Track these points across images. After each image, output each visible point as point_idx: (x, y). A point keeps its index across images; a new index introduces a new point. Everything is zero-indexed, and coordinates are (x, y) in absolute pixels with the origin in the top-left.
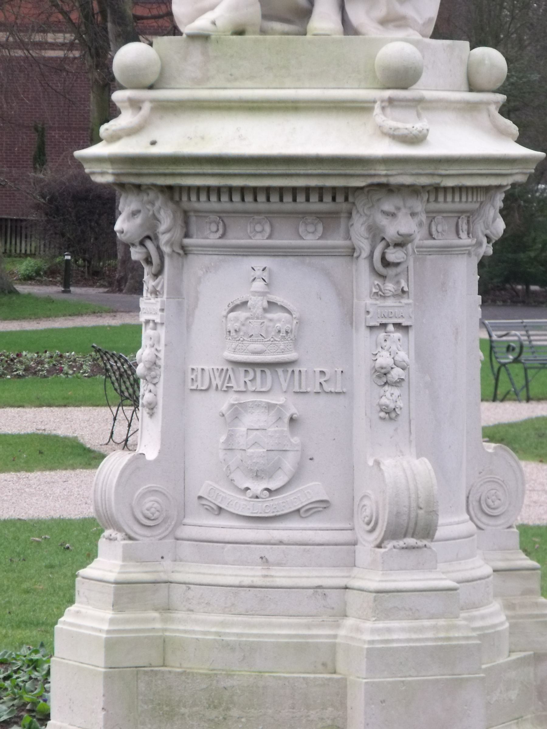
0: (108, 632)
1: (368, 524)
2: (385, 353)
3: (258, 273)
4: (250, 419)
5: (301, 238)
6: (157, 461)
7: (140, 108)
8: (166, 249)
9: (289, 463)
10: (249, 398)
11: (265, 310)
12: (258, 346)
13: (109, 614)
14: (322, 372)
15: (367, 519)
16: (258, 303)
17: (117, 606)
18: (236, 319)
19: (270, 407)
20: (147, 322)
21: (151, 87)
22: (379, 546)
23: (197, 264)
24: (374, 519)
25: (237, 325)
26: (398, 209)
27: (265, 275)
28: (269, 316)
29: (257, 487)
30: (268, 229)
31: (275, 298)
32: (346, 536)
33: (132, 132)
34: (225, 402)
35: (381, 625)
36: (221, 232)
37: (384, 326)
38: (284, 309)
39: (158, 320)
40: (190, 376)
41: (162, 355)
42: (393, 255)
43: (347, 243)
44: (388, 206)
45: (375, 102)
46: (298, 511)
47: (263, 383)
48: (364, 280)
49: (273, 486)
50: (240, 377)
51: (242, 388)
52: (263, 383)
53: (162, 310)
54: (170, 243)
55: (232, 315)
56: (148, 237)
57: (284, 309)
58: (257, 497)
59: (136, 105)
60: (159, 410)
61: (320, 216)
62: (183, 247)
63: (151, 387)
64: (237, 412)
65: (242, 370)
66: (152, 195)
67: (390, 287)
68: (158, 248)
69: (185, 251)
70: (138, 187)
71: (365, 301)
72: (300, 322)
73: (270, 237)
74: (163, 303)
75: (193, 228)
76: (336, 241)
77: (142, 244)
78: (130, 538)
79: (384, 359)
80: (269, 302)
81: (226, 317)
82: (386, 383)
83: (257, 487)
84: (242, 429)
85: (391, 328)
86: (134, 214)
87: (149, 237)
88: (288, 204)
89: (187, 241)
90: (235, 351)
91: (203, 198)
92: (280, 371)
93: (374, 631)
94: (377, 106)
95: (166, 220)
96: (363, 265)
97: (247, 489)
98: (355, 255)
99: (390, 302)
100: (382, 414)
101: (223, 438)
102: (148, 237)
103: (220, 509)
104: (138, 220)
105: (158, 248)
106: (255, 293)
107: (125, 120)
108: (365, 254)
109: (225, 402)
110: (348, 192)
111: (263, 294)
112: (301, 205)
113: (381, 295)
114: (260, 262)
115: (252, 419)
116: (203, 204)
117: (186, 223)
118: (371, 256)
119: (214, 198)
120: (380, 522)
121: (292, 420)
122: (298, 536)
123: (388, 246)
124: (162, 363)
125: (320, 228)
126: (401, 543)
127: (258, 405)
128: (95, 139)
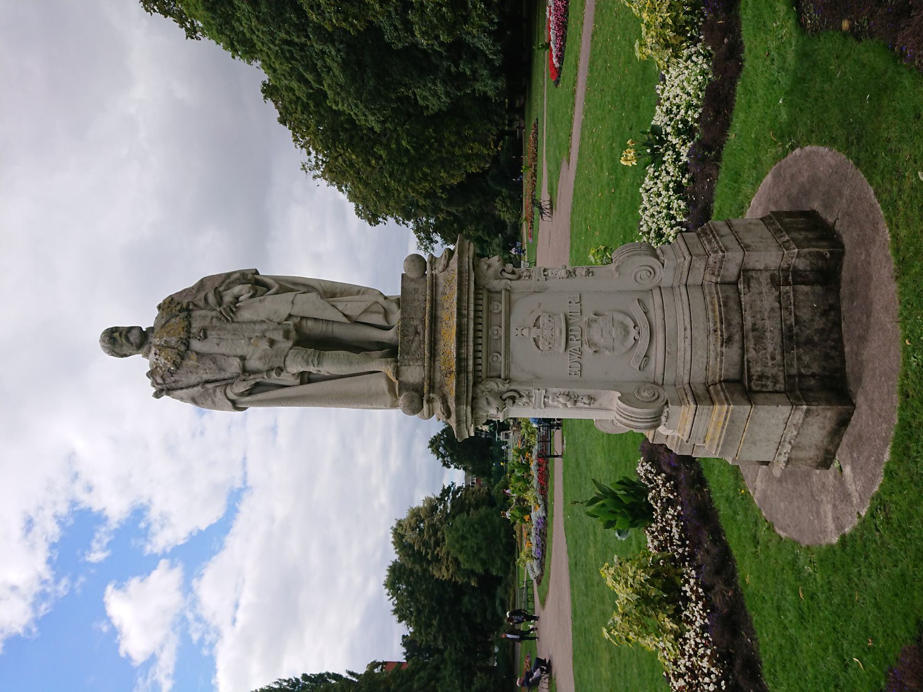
0: (729, 404)
3: (519, 332)
4: (596, 337)
9: (620, 317)
11: (539, 328)
16: (535, 332)
18: (543, 344)
22: (663, 265)
24: (649, 268)
25: (547, 343)
29: (633, 333)
32: (656, 292)
41: (562, 390)
43: (503, 292)
50: (575, 344)
66: (479, 391)
69: (507, 379)
70: (473, 398)
71: (533, 283)
77: (505, 400)
78: (667, 403)
83: (633, 333)
86: (488, 403)
90: (560, 345)
92: (571, 322)
95: (492, 385)
99: (533, 275)
101: (607, 353)
104: (491, 399)
106: (530, 334)
113: (530, 276)
116: (483, 368)
118: (510, 280)
120: (651, 264)
122: (659, 312)
123: (504, 270)
124: (566, 390)
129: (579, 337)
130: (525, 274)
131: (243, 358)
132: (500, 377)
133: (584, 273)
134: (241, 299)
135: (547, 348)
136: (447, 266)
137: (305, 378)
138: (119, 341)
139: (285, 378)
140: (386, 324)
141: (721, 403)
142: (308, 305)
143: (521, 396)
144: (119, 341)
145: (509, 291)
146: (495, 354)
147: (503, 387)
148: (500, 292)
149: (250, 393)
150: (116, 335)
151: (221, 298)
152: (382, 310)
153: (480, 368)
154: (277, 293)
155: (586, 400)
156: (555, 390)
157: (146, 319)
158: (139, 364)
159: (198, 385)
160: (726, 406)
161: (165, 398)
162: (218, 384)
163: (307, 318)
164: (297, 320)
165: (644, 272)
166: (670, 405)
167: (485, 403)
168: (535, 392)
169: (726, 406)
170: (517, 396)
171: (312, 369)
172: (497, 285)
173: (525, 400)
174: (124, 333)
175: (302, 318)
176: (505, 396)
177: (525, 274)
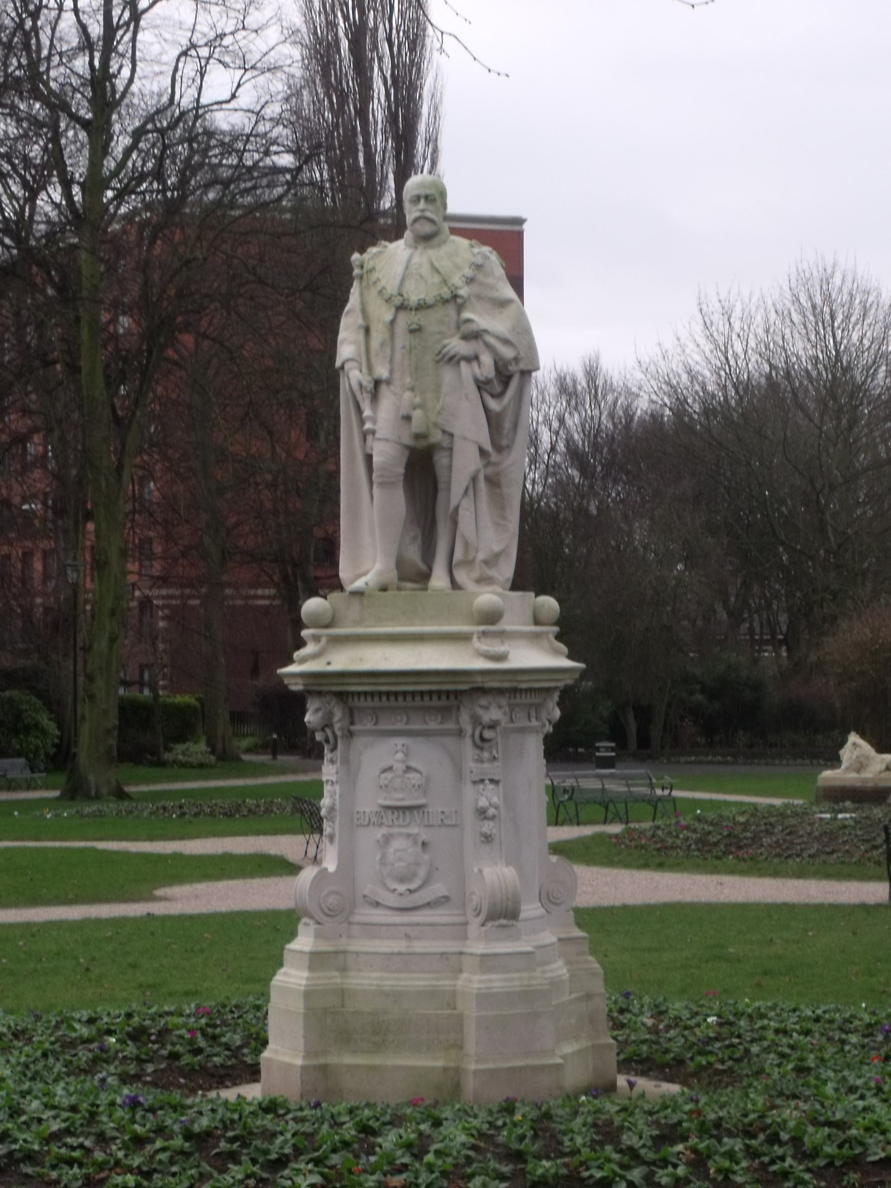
5: (427, 724)
6: (336, 872)
7: (319, 641)
8: (339, 733)
9: (422, 873)
10: (396, 830)
11: (405, 772)
12: (400, 796)
13: (306, 974)
14: (443, 813)
16: (399, 767)
17: (311, 968)
19: (409, 835)
20: (327, 781)
21: (327, 626)
22: (483, 925)
23: (359, 742)
25: (386, 782)
26: (490, 703)
27: (404, 749)
30: (405, 719)
33: (315, 656)
34: (380, 833)
35: (485, 977)
37: (482, 781)
38: (416, 771)
39: (334, 779)
40: (356, 816)
41: (337, 803)
42: (488, 734)
44: (483, 702)
45: (473, 634)
47: (404, 819)
48: (469, 751)
49: (412, 886)
50: (390, 816)
52: (404, 819)
54: (341, 729)
55: (383, 776)
56: (327, 726)
57: (416, 771)
59: (316, 638)
61: (438, 709)
64: (387, 839)
65: (390, 812)
66: (328, 697)
67: (486, 755)
68: (333, 733)
69: (351, 734)
71: (470, 764)
72: (428, 780)
73: (407, 723)
75: (356, 719)
76: (450, 725)
77: (323, 730)
78: (319, 923)
79: (483, 802)
83: (402, 888)
84: (391, 850)
85: (487, 782)
87: (327, 725)
88: (418, 702)
89: (352, 728)
90: (385, 799)
91: (362, 699)
92: (415, 812)
93: (480, 982)
95: (338, 714)
96: (468, 741)
97: (395, 890)
99: (486, 765)
101: (378, 857)
102: (327, 726)
104: (320, 714)
105: (333, 733)
107: (310, 649)
108: (469, 733)
109: (380, 833)
110: (457, 694)
111: (403, 761)
112: (427, 702)
113: (480, 760)
114: (400, 741)
115: (398, 844)
116: (362, 703)
117: (352, 716)
118: (473, 735)
119: (369, 699)
122: (429, 920)
124: (337, 807)
125: (439, 717)
126: (497, 923)
127: (401, 834)
128: (290, 661)
129: (396, 822)
131: (388, 382)
132: (352, 723)
133: (484, 830)
147: (337, 726)
148: (458, 722)
152: (470, 557)
163: (451, 456)
164: (445, 444)
175: (451, 449)
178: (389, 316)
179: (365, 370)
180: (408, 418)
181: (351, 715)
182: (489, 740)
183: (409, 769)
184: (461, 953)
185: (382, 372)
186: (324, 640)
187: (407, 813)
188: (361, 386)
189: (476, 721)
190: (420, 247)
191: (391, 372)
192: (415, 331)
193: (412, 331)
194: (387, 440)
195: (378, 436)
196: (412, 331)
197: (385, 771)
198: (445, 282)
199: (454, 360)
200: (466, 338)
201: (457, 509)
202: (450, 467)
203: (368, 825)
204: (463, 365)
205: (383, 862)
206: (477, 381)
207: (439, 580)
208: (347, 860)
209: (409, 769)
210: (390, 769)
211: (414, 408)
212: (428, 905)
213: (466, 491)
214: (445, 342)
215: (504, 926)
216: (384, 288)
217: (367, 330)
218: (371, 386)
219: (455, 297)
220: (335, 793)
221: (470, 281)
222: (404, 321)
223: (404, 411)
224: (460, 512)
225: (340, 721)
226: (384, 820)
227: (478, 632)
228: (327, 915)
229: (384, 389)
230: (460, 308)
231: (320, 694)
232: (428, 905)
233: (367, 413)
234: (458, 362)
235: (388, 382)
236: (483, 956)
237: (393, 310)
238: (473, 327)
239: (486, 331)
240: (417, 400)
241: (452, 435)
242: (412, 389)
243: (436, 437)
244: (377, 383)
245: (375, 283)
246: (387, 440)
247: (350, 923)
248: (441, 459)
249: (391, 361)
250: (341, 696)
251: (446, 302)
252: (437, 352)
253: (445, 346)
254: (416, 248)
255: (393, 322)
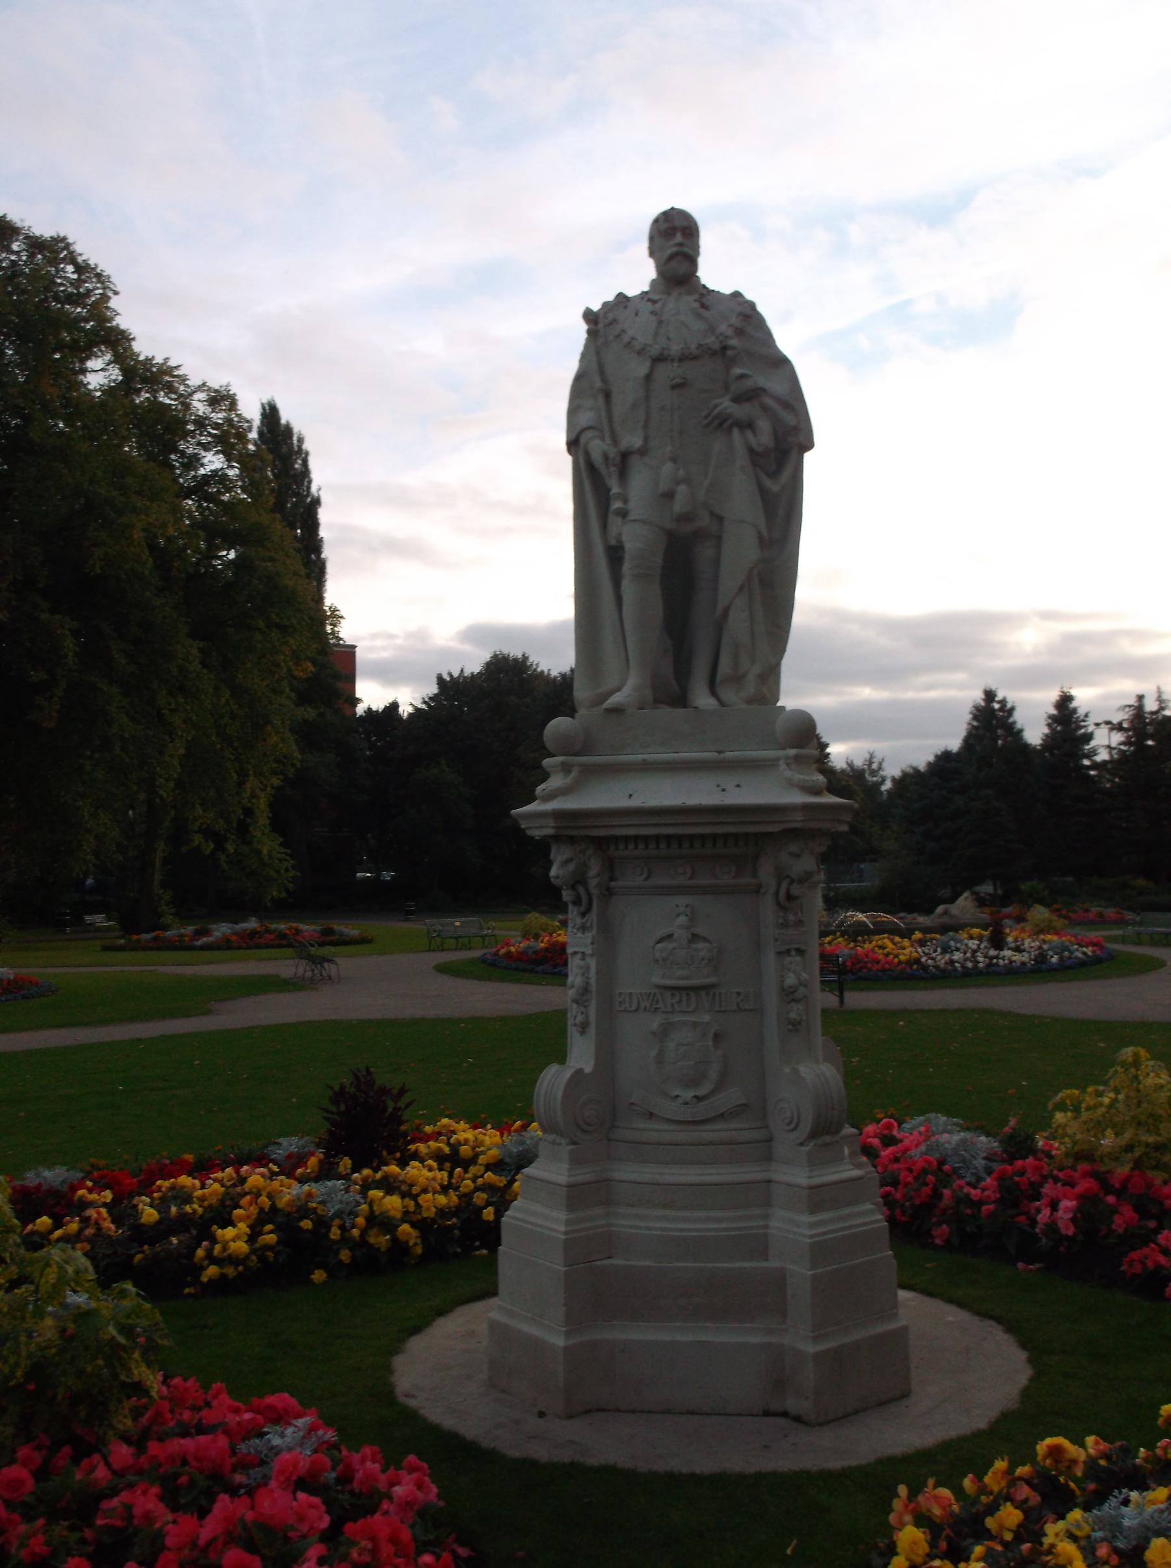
0: (566, 1233)
1: (789, 1124)
2: (791, 975)
3: (682, 909)
7: (570, 772)
8: (595, 892)
10: (676, 1018)
13: (563, 1216)
14: (738, 994)
15: (787, 1121)
17: (570, 1208)
19: (695, 1025)
20: (575, 953)
22: (801, 1144)
24: (795, 1121)
28: (694, 946)
29: (689, 1095)
30: (689, 870)
31: (699, 931)
34: (655, 1022)
36: (645, 876)
37: (788, 951)
38: (705, 939)
39: (589, 951)
41: (593, 981)
42: (795, 890)
44: (794, 848)
45: (778, 759)
46: (722, 1115)
48: (768, 910)
49: (701, 1092)
51: (669, 1009)
53: (592, 943)
56: (578, 882)
57: (705, 939)
58: (686, 1104)
59: (566, 768)
60: (592, 1029)
62: (608, 889)
63: (583, 1009)
65: (668, 994)
68: (587, 890)
69: (608, 893)
74: (593, 937)
77: (573, 888)
78: (574, 1143)
79: (791, 980)
80: (694, 935)
81: (653, 948)
82: (793, 1000)
83: (689, 1095)
85: (793, 953)
87: (578, 880)
89: (613, 884)
90: (663, 977)
92: (703, 993)
93: (812, 1225)
94: (782, 762)
96: (769, 900)
98: (763, 891)
100: (790, 1027)
101: (654, 1053)
102: (578, 882)
103: (651, 1114)
104: (571, 867)
105: (587, 890)
107: (556, 781)
109: (655, 1022)
110: (760, 839)
113: (785, 925)
114: (682, 900)
121: (716, 1035)
123: (793, 881)
124: (593, 987)
128: (531, 798)
129: (677, 1008)
130: (791, 917)
131: (643, 452)
132: (612, 879)
133: (793, 1015)
134: (749, 434)
135: (657, 955)
136: (791, 784)
137: (615, 554)
138: (675, 237)
139: (615, 523)
140: (719, 677)
141: (568, 1222)
142: (740, 552)
143: (583, 915)
144: (675, 237)
145: (758, 890)
146: (646, 870)
147: (593, 883)
148: (755, 874)
149: (591, 468)
150: (679, 238)
151: (749, 399)
153: (622, 847)
154: (763, 492)
155: (580, 1018)
156: (593, 971)
157: (716, 271)
158: (637, 274)
159: (604, 380)
160: (562, 1228)
161: (583, 327)
162: (603, 414)
163: (718, 547)
165: (788, 1113)
166: (570, 1147)
167: (565, 857)
168: (589, 936)
169: (562, 1228)
170: (583, 909)
171: (626, 567)
172: (766, 871)
173: (579, 921)
174: (685, 249)
175: (719, 539)
176: (581, 889)
177: (791, 917)
178: (643, 370)
179: (608, 441)
180: (669, 495)
181: (611, 869)
182: (796, 898)
183: (695, 938)
184: (769, 1181)
185: (634, 441)
186: (574, 774)
187: (692, 994)
188: (606, 457)
189: (781, 875)
190: (675, 294)
191: (646, 439)
192: (679, 386)
193: (674, 387)
194: (644, 522)
195: (632, 517)
196: (674, 387)
197: (660, 941)
198: (712, 329)
199: (723, 424)
200: (737, 399)
201: (726, 611)
202: (717, 561)
203: (637, 1009)
204: (736, 432)
205: (660, 1060)
206: (752, 452)
207: (703, 700)
208: (607, 1053)
209: (695, 938)
210: (670, 937)
211: (678, 483)
212: (722, 1116)
213: (741, 588)
214: (717, 401)
215: (826, 1145)
216: (633, 338)
217: (608, 396)
218: (618, 459)
219: (725, 348)
220: (588, 968)
221: (740, 332)
222: (666, 373)
223: (663, 487)
224: (732, 613)
225: (598, 875)
226: (660, 1005)
227: (787, 758)
228: (585, 1132)
229: (635, 462)
230: (730, 363)
231: (572, 840)
232: (722, 1116)
233: (615, 489)
234: (729, 431)
235: (643, 452)
236: (811, 1188)
237: (648, 364)
238: (749, 384)
239: (763, 390)
240: (681, 473)
241: (720, 519)
242: (674, 460)
243: (704, 520)
244: (625, 456)
245: (618, 337)
246: (644, 522)
247: (609, 1140)
248: (705, 552)
249: (646, 426)
250: (601, 843)
251: (714, 353)
252: (705, 413)
253: (716, 406)
254: (669, 294)
255: (648, 378)
